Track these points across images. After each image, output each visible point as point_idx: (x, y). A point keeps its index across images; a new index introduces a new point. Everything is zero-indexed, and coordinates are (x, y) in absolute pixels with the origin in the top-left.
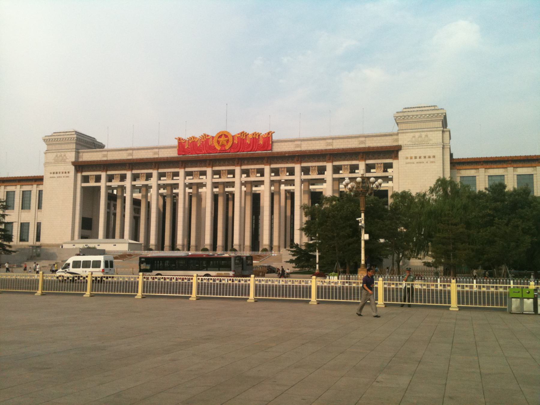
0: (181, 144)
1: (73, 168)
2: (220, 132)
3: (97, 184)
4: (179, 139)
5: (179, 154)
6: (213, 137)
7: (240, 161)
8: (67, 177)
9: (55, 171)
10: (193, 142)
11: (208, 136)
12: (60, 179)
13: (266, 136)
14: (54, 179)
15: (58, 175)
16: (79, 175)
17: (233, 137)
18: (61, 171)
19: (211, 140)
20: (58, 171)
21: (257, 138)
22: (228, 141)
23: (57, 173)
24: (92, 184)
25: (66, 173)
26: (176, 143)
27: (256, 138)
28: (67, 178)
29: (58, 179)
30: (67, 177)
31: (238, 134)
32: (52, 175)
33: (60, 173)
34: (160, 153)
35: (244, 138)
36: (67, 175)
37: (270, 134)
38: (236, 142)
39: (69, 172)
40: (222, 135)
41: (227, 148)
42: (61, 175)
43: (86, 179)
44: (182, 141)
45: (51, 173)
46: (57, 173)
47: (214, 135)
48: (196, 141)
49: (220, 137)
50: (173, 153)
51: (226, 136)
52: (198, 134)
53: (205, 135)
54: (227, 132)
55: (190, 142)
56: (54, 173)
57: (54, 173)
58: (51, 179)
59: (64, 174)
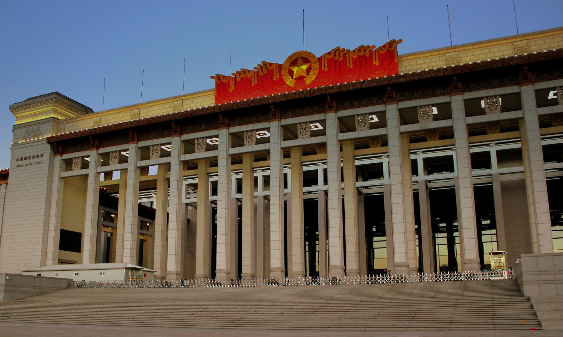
0: (222, 84)
2: (294, 55)
3: (84, 172)
4: (218, 78)
6: (280, 66)
8: (40, 163)
9: (24, 156)
10: (243, 79)
11: (271, 64)
12: (30, 167)
13: (385, 51)
14: (22, 168)
15: (28, 161)
16: (58, 159)
17: (320, 59)
18: (31, 155)
20: (28, 155)
21: (367, 55)
23: (26, 158)
24: (77, 171)
25: (38, 157)
26: (212, 84)
27: (364, 57)
28: (40, 165)
29: (27, 167)
30: (40, 163)
31: (329, 53)
32: (19, 163)
35: (341, 59)
36: (40, 159)
37: (391, 46)
39: (42, 156)
40: (297, 60)
42: (31, 161)
44: (225, 81)
45: (18, 160)
46: (26, 158)
47: (282, 63)
48: (249, 77)
50: (208, 102)
52: (251, 65)
53: (265, 64)
54: (305, 52)
55: (238, 79)
56: (22, 159)
58: (18, 169)
59: (36, 160)
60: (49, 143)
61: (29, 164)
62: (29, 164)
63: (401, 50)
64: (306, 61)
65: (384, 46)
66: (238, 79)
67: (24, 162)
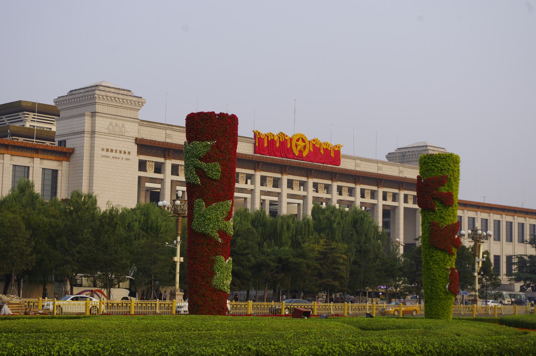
1: (135, 147)
5: (255, 153)
7: (309, 172)
8: (127, 159)
9: (110, 148)
12: (117, 160)
14: (108, 159)
15: (114, 154)
18: (119, 149)
19: (289, 142)
21: (329, 149)
22: (305, 147)
23: (112, 151)
25: (125, 153)
29: (114, 160)
30: (127, 159)
32: (105, 153)
33: (116, 151)
34: (164, 135)
35: (318, 146)
36: (127, 156)
38: (312, 150)
39: (129, 153)
41: (305, 154)
42: (118, 155)
43: (142, 166)
45: (103, 150)
49: (298, 140)
51: (303, 141)
57: (107, 150)
58: (104, 159)
59: (122, 155)
60: (136, 143)
61: (116, 158)
62: (116, 158)
63: (343, 152)
64: (303, 141)
65: (336, 146)
66: (269, 139)
67: (109, 154)
